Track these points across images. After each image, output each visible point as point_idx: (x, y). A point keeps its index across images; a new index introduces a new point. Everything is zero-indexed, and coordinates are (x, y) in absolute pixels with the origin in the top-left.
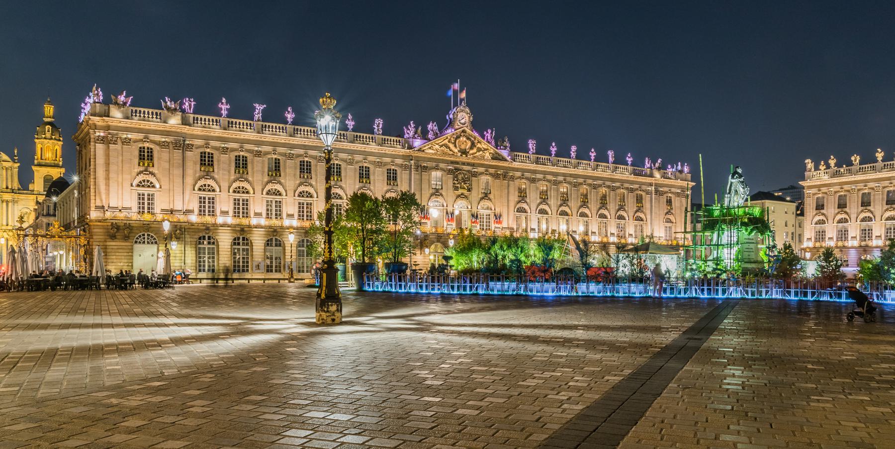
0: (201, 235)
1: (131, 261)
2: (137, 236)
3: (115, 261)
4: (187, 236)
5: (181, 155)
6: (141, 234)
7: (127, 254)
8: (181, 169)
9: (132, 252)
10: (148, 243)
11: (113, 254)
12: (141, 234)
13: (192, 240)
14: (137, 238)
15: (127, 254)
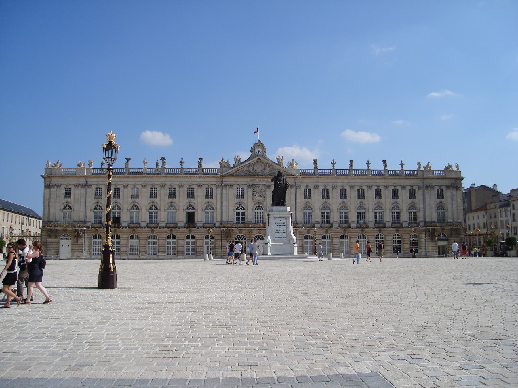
0: (93, 234)
1: (58, 249)
2: (62, 235)
3: (50, 249)
4: (86, 235)
5: (85, 191)
6: (64, 234)
7: (56, 245)
8: (85, 198)
9: (59, 244)
10: (67, 239)
11: (50, 245)
12: (64, 234)
13: (88, 237)
14: (62, 237)
15: (56, 245)
